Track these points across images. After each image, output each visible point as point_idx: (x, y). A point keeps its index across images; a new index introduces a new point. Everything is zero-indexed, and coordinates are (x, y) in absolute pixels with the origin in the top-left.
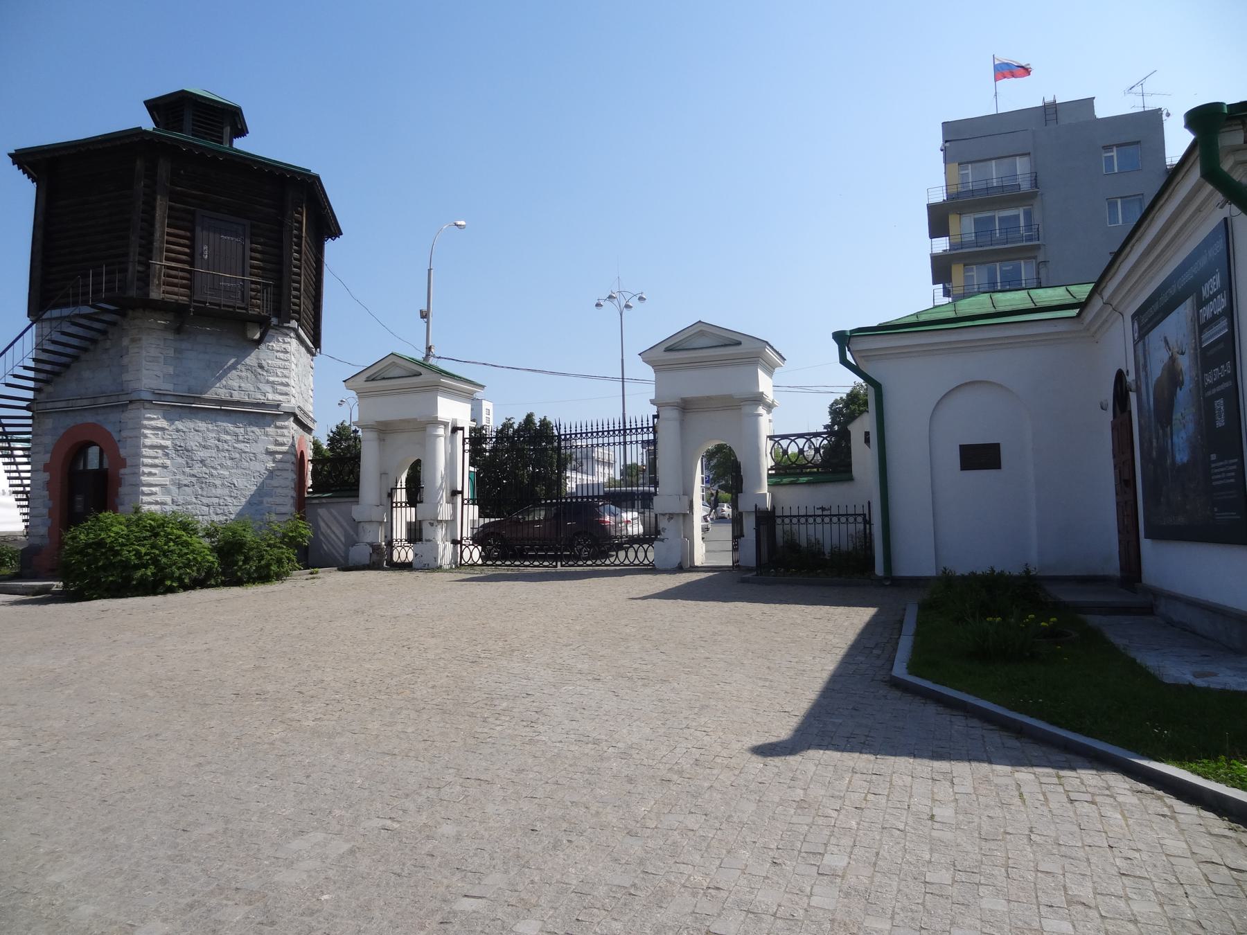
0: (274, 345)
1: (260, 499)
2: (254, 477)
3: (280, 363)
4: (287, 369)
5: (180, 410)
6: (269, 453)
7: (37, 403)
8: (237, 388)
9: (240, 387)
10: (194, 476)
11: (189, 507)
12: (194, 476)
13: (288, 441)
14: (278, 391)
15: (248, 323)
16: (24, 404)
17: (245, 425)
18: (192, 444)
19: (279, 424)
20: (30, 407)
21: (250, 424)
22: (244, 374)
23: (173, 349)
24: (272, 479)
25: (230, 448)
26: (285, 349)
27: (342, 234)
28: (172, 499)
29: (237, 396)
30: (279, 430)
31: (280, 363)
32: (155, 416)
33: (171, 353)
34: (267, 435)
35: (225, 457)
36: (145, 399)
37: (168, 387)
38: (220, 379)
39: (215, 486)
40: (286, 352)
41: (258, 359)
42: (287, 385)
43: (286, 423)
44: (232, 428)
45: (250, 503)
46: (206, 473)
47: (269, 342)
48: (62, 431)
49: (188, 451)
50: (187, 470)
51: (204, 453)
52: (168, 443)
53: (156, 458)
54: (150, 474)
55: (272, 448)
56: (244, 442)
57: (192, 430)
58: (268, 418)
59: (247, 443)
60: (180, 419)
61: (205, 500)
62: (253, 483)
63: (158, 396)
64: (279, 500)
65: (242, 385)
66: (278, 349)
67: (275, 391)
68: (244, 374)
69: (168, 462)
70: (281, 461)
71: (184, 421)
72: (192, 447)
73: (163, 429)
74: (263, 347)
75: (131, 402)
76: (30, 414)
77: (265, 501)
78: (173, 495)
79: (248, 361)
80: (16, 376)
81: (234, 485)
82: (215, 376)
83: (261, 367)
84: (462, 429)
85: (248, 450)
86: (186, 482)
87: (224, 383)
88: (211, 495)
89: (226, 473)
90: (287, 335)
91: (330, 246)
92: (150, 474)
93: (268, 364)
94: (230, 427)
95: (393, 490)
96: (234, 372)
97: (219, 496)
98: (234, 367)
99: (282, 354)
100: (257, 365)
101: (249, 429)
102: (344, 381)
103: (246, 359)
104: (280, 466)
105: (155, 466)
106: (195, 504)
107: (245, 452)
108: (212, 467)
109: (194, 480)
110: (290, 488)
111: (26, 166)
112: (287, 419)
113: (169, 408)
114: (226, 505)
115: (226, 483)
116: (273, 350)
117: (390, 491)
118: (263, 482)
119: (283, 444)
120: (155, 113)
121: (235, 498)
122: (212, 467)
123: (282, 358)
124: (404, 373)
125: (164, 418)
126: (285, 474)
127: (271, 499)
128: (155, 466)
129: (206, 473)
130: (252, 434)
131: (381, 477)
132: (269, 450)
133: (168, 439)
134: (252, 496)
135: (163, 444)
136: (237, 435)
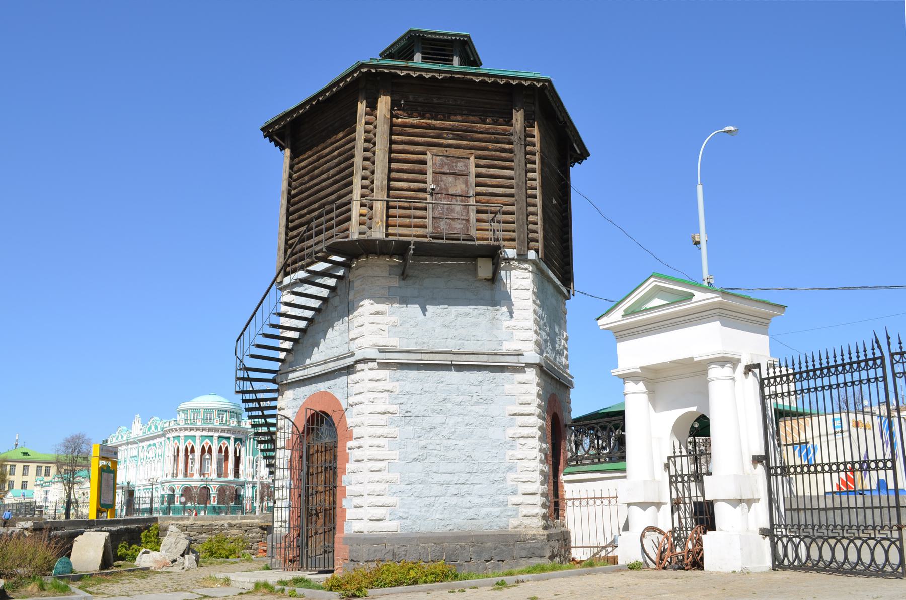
1: (503, 475)
7: (281, 374)
12: (424, 447)
15: (479, 258)
16: (270, 376)
20: (275, 380)
27: (589, 155)
36: (368, 357)
44: (465, 387)
48: (300, 403)
61: (438, 478)
76: (275, 387)
77: (508, 479)
80: (258, 346)
91: (577, 172)
111: (276, 138)
115: (462, 456)
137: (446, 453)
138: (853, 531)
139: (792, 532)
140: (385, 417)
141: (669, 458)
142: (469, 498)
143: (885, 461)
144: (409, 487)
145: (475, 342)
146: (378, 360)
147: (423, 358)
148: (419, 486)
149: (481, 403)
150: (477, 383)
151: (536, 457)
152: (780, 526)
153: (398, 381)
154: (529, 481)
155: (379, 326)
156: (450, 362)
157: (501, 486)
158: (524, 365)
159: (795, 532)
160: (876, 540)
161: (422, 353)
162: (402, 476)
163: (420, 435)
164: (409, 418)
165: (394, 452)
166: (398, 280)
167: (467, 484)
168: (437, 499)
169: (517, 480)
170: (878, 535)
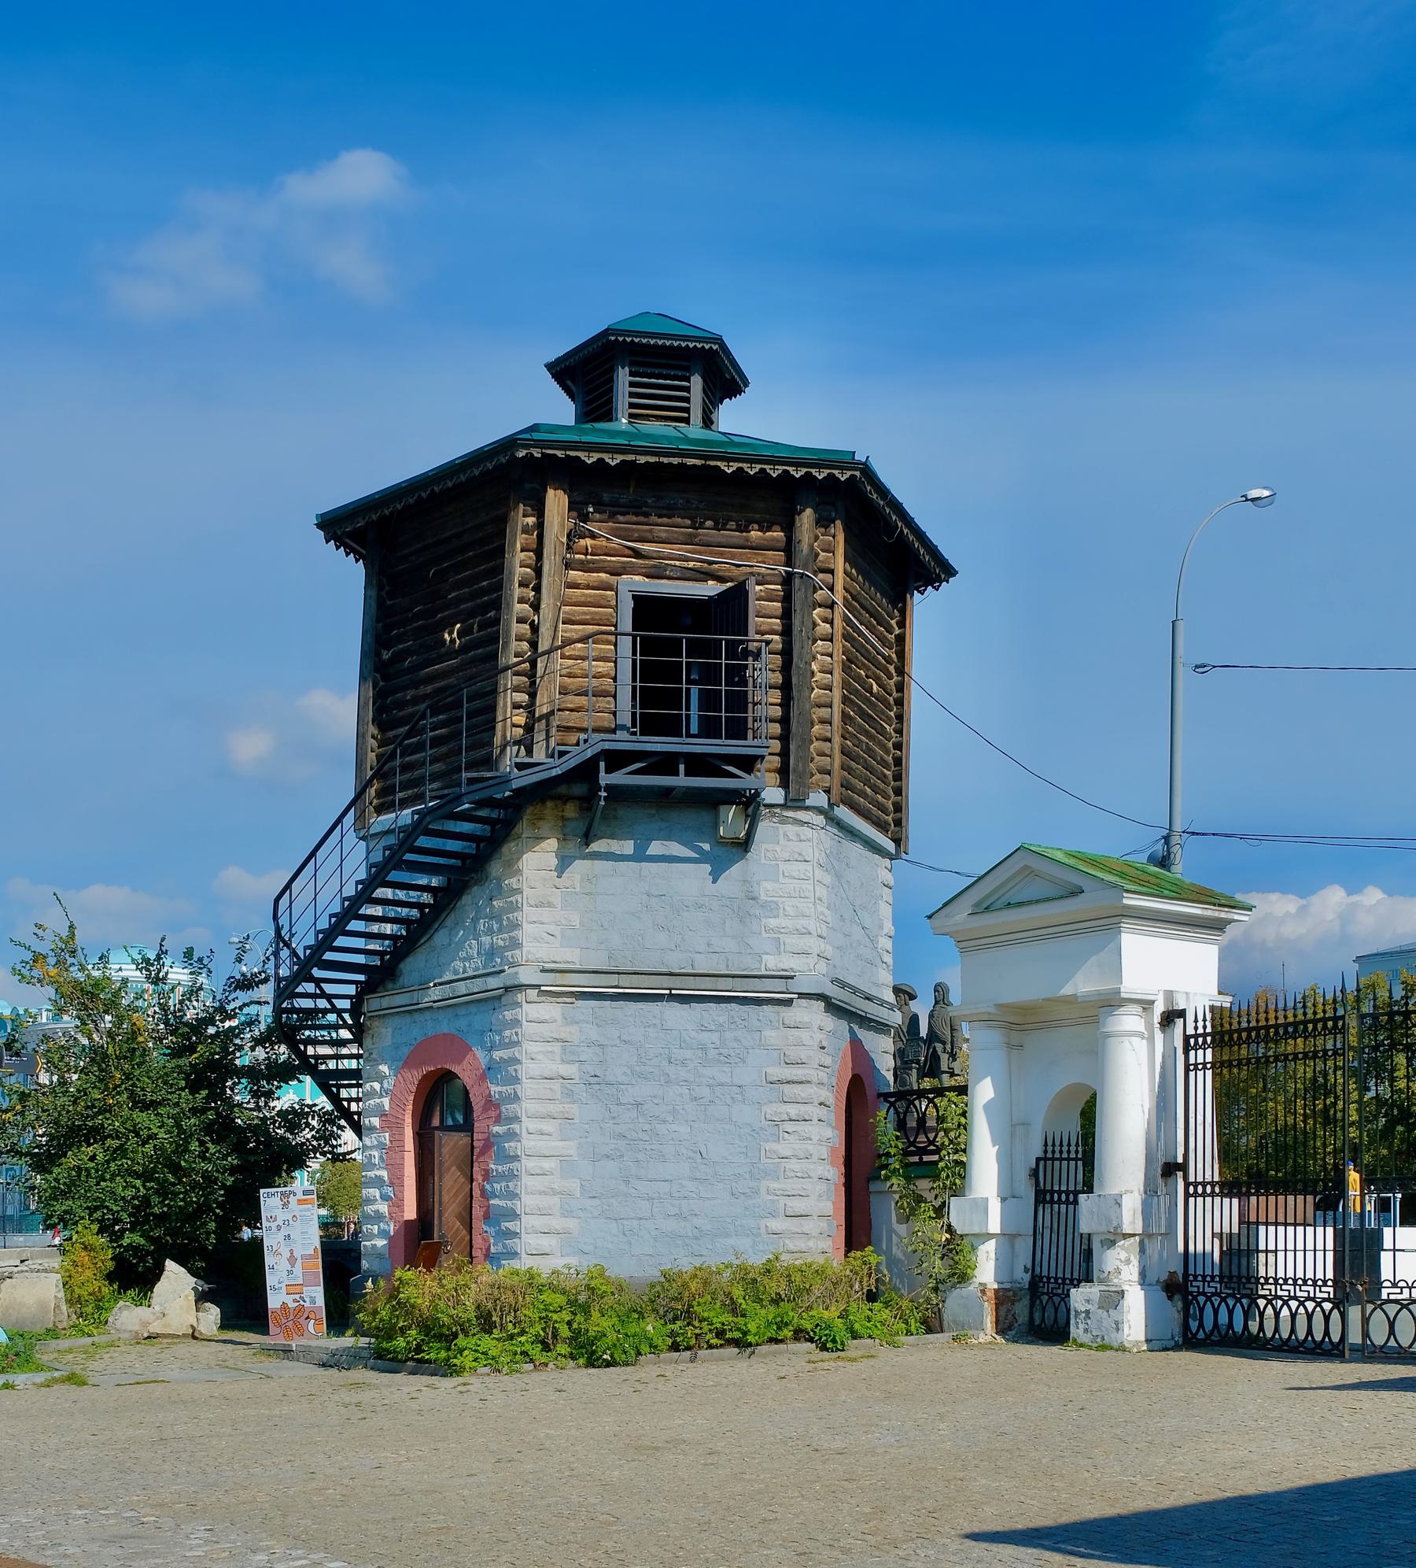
14: (788, 948)
35: (681, 1095)
37: (571, 956)
44: (694, 1034)
57: (618, 1041)
64: (791, 1186)
66: (786, 856)
69: (573, 1109)
75: (507, 989)
77: (763, 1191)
84: (1182, 1014)
95: (1042, 1163)
102: (930, 917)
111: (348, 541)
115: (685, 1152)
117: (1034, 1166)
120: (569, 383)
123: (793, 874)
124: (1051, 891)
127: (774, 1185)
131: (1013, 1134)
136: (704, 1049)
138: (1232, 1285)
139: (1230, 1288)
140: (556, 1086)
141: (1038, 1160)
142: (696, 1221)
143: (1196, 1195)
146: (543, 988)
147: (621, 984)
148: (612, 1200)
149: (719, 1061)
150: (713, 1028)
152: (1195, 1279)
153: (577, 1023)
155: (546, 928)
156: (667, 992)
157: (750, 1202)
159: (1234, 1289)
160: (1315, 1302)
161: (618, 973)
163: (615, 1115)
164: (598, 1087)
165: (572, 1143)
167: (693, 1198)
168: (643, 1222)
169: (778, 1193)
170: (1318, 1295)
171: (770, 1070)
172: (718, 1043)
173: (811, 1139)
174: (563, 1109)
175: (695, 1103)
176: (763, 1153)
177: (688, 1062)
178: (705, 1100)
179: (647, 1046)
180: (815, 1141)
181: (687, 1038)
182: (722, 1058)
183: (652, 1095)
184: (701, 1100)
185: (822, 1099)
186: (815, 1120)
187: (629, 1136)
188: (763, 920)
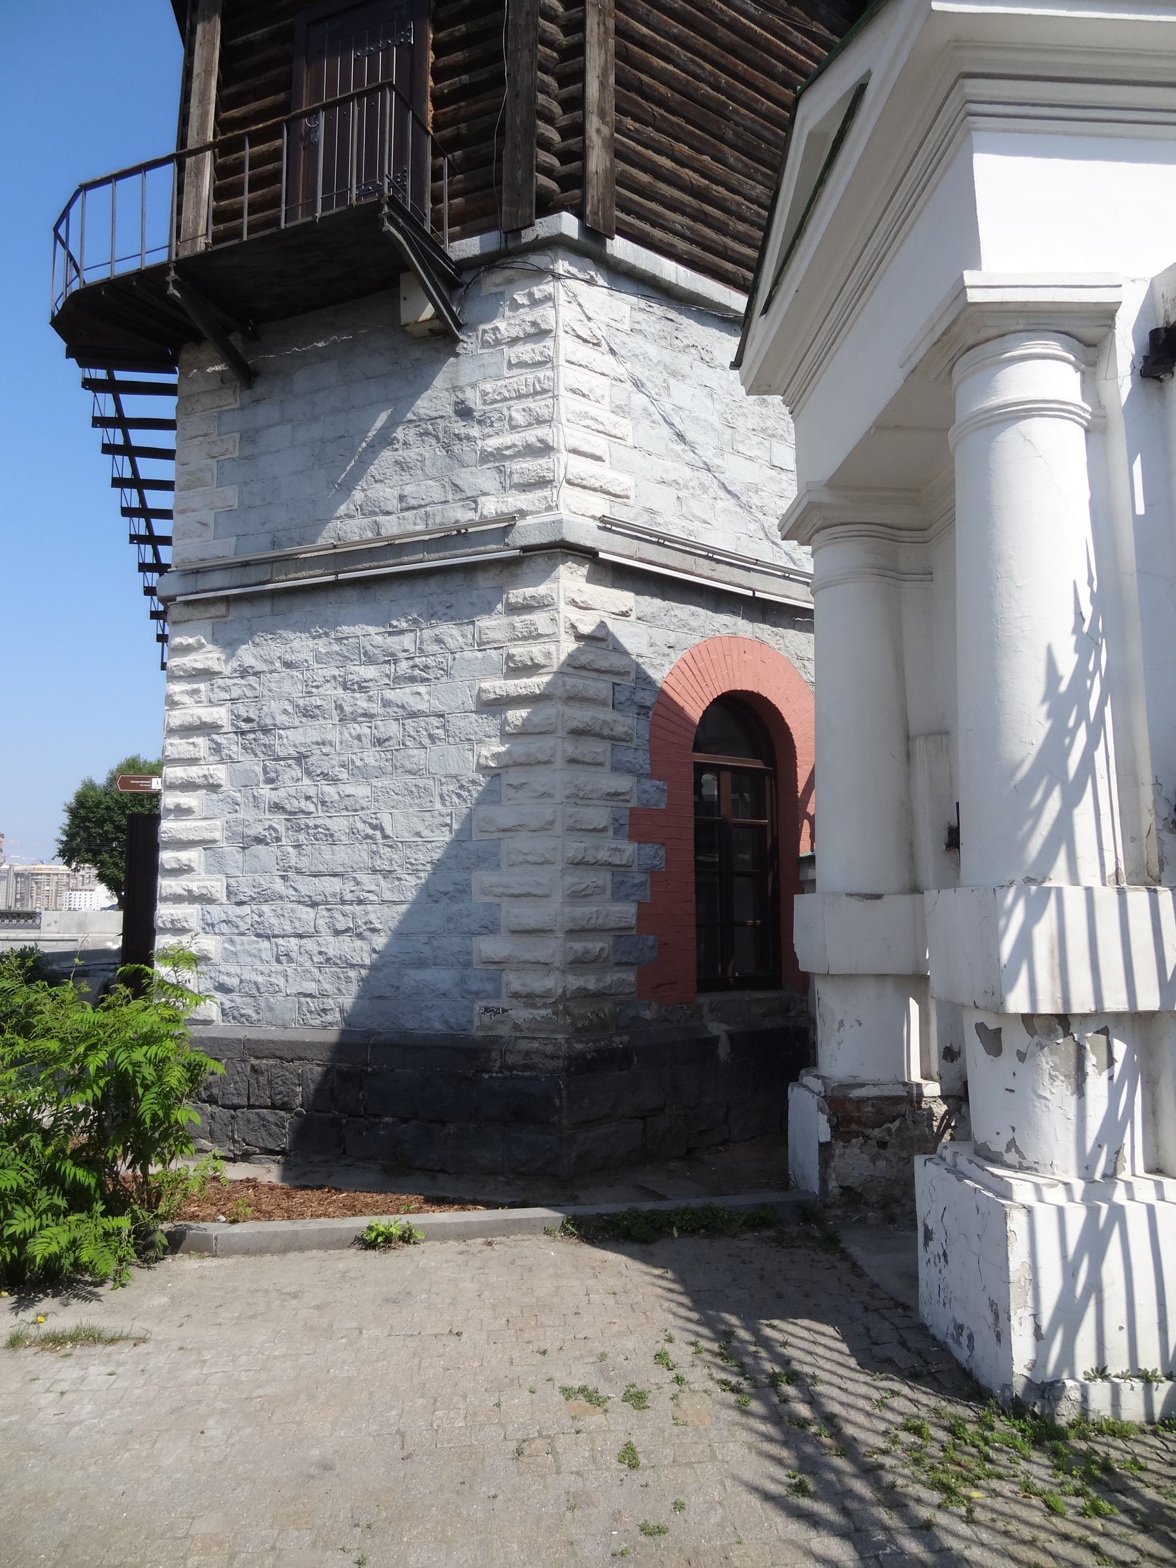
0: (505, 325)
1: (460, 876)
2: (442, 797)
3: (522, 379)
4: (544, 391)
5: (246, 610)
6: (493, 706)
8: (393, 504)
9: (402, 498)
10: (277, 807)
11: (265, 908)
12: (277, 807)
13: (548, 655)
14: (516, 479)
17: (415, 621)
18: (274, 710)
19: (517, 595)
21: (432, 615)
22: (411, 454)
23: (237, 435)
24: (498, 802)
25: (376, 708)
26: (534, 324)
28: (228, 886)
29: (391, 526)
30: (517, 620)
31: (522, 379)
32: (191, 641)
33: (231, 446)
34: (482, 645)
35: (359, 738)
37: (223, 548)
38: (346, 489)
39: (330, 837)
40: (540, 334)
41: (454, 388)
42: (545, 449)
43: (542, 589)
44: (379, 640)
45: (429, 895)
46: (308, 798)
47: (490, 319)
49: (266, 731)
50: (266, 792)
51: (305, 735)
52: (220, 715)
53: (193, 761)
54: (181, 812)
55: (498, 686)
56: (412, 679)
57: (278, 665)
58: (484, 581)
59: (424, 680)
60: (248, 635)
61: (307, 886)
62: (441, 820)
63: (192, 578)
65: (408, 490)
66: (515, 332)
67: (509, 485)
68: (411, 454)
69: (220, 773)
70: (524, 732)
71: (257, 640)
72: (273, 718)
73: (206, 674)
74: (469, 344)
77: (475, 889)
78: (230, 871)
79: (424, 405)
81: (382, 829)
82: (334, 482)
83: (464, 412)
85: (423, 707)
86: (257, 830)
87: (358, 496)
88: (322, 868)
89: (361, 791)
90: (542, 273)
92: (181, 812)
93: (484, 394)
94: (372, 635)
96: (387, 455)
97: (341, 869)
98: (385, 440)
99: (529, 347)
100: (449, 410)
101: (427, 634)
103: (419, 402)
104: (524, 748)
105: (188, 786)
106: (281, 898)
107: (414, 715)
108: (325, 775)
109: (278, 821)
110: (558, 829)
112: (546, 574)
113: (220, 609)
114: (360, 902)
115: (360, 826)
116: (498, 342)
118: (469, 817)
119: (532, 668)
121: (385, 874)
122: (325, 775)
123: (526, 358)
125: (215, 641)
126: (540, 779)
128: (188, 786)
129: (308, 798)
130: (436, 648)
132: (484, 696)
133: (220, 703)
134: (438, 866)
135: (207, 719)
137: (328, 822)
144: (246, 909)
145: (406, 514)
151: (552, 823)
154: (528, 895)
157: (455, 907)
158: (517, 552)
162: (231, 881)
164: (252, 736)
166: (238, 391)
167: (372, 903)
168: (304, 941)
169: (498, 891)
171: (485, 685)
172: (412, 649)
173: (550, 796)
174: (207, 773)
175: (378, 749)
176: (474, 824)
177: (370, 684)
178: (391, 743)
179: (316, 666)
180: (558, 798)
181: (369, 648)
182: (417, 672)
183: (319, 740)
184: (387, 743)
185: (574, 724)
186: (559, 762)
187: (288, 807)
188: (479, 443)
